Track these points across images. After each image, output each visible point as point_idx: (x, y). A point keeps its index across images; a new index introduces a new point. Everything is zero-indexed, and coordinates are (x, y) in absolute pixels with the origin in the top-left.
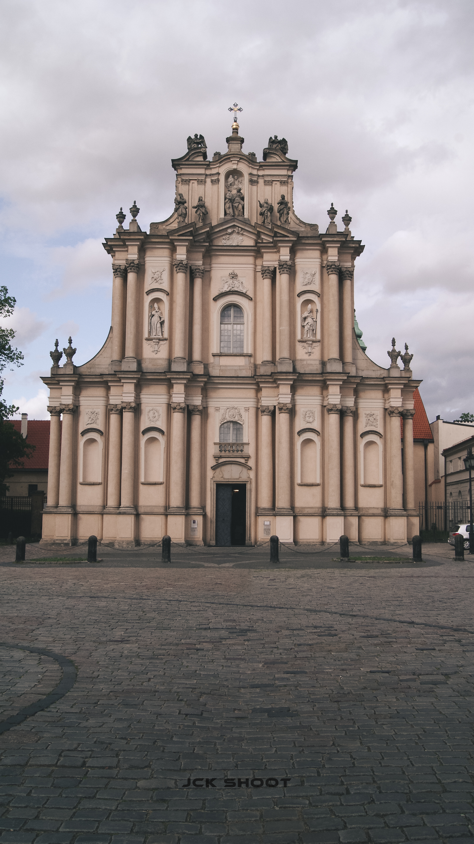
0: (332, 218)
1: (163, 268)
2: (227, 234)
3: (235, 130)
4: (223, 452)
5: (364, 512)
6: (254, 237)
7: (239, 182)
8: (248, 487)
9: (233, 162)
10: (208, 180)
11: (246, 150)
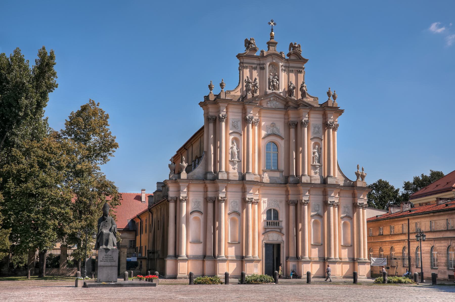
0: (329, 96)
1: (238, 120)
2: (270, 101)
3: (272, 37)
4: (269, 226)
5: (343, 260)
6: (284, 103)
7: (275, 69)
8: (282, 245)
9: (273, 58)
10: (258, 67)
11: (278, 49)
